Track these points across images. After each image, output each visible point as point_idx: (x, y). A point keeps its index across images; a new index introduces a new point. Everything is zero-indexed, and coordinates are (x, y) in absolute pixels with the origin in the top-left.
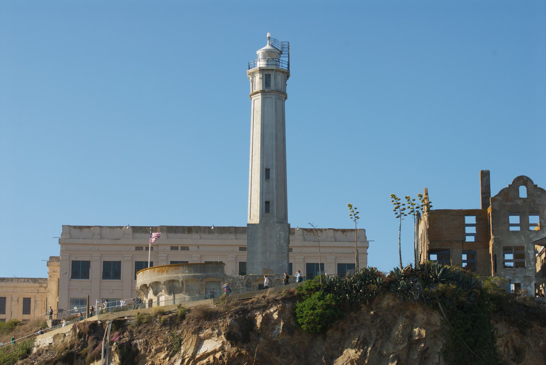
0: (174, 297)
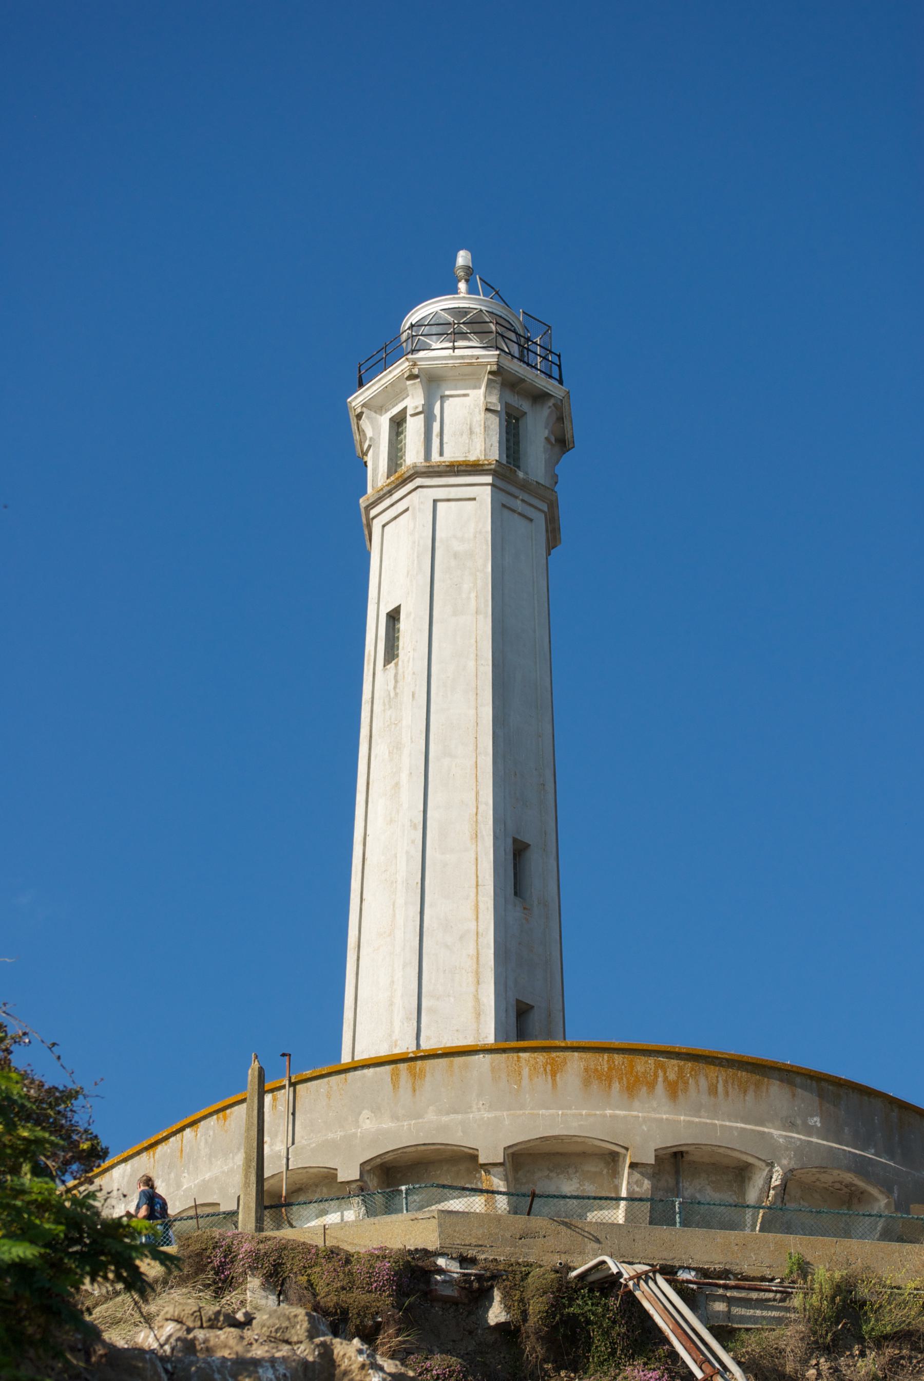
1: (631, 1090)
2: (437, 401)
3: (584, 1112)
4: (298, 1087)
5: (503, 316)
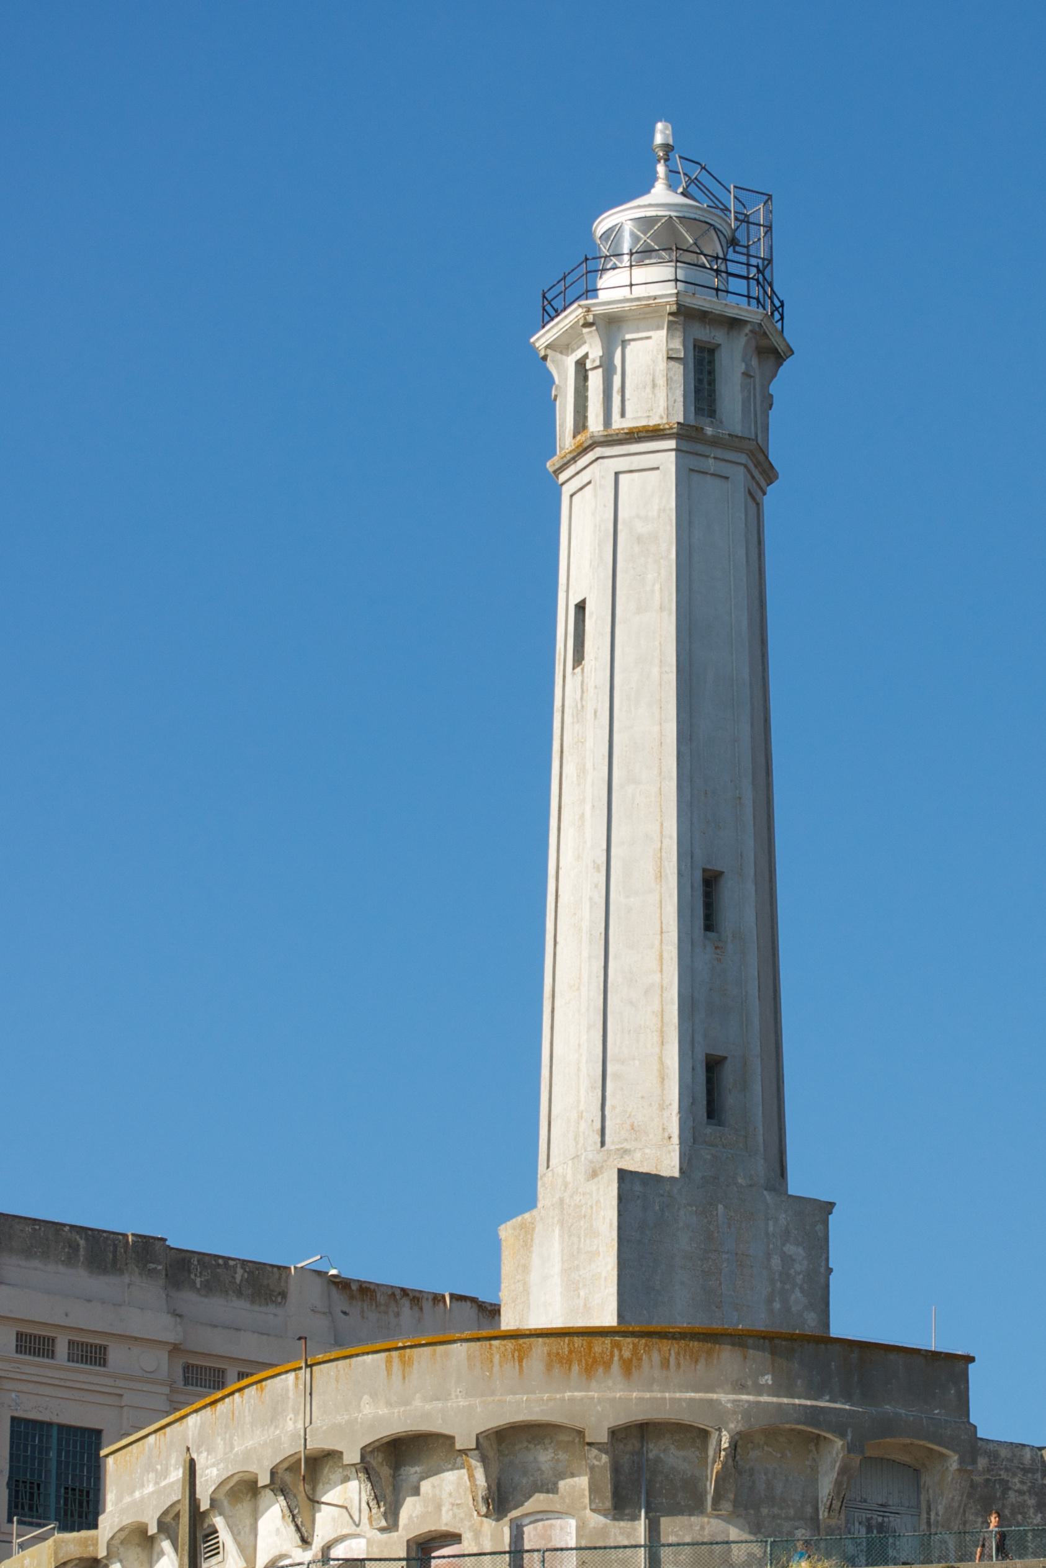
0: (653, 1529)
1: (589, 1371)
2: (616, 349)
3: (546, 1396)
4: (314, 1368)
5: (697, 217)
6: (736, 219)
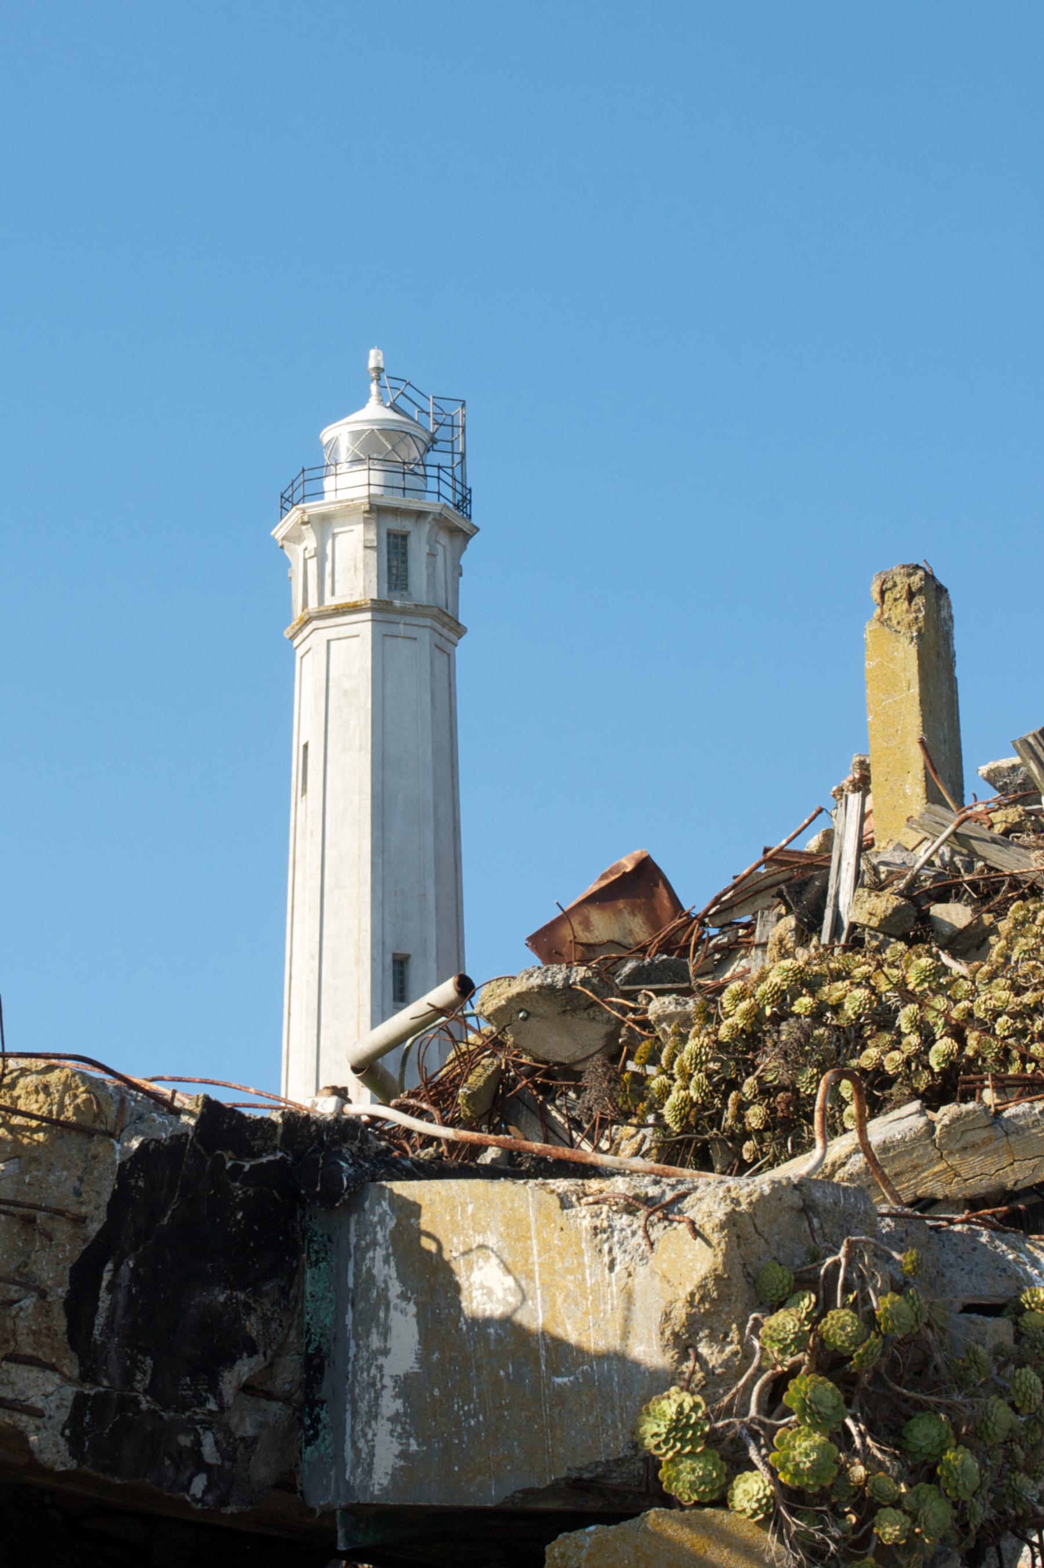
6: (436, 423)
